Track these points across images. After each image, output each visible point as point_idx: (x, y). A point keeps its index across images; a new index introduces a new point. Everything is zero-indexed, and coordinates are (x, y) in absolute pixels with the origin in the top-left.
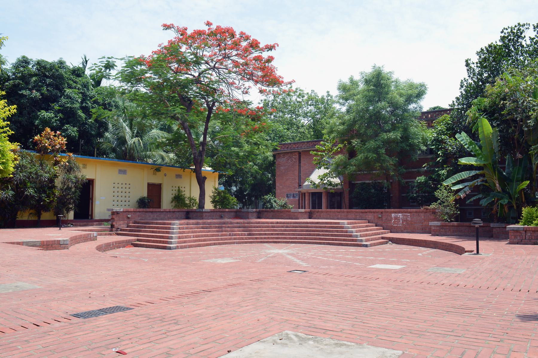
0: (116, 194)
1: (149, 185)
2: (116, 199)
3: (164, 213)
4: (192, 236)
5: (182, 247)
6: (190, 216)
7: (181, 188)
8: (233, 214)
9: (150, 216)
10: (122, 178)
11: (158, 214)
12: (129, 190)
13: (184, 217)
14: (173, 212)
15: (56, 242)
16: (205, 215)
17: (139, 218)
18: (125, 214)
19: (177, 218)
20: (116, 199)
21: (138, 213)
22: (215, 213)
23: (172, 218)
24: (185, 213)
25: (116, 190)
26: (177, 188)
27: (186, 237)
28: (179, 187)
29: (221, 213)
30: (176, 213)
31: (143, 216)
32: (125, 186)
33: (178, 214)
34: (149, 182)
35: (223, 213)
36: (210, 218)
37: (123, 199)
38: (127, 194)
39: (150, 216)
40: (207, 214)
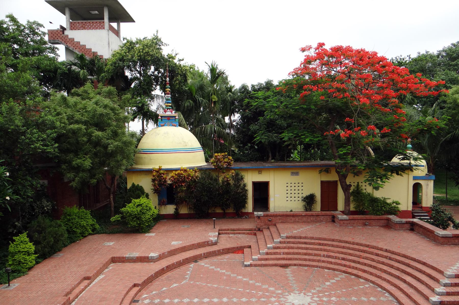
0: (289, 192)
1: (322, 182)
2: (289, 195)
3: (306, 217)
4: (282, 253)
5: (256, 266)
6: (335, 220)
7: (360, 184)
8: (383, 221)
9: (291, 220)
10: (295, 179)
11: (300, 217)
12: (302, 188)
13: (331, 220)
14: (317, 216)
15: (146, 258)
16: (342, 223)
17: (281, 221)
18: (266, 217)
19: (322, 221)
20: (289, 195)
21: (279, 217)
22: (357, 220)
23: (316, 221)
24: (331, 216)
25: (289, 188)
26: (356, 184)
27: (275, 253)
28: (358, 183)
29: (365, 221)
30: (320, 216)
31: (284, 219)
32: (289, 187)
33: (323, 217)
34: (322, 180)
35: (368, 221)
36: (349, 225)
37: (296, 195)
38: (300, 192)
39: (291, 220)
40: (346, 222)
